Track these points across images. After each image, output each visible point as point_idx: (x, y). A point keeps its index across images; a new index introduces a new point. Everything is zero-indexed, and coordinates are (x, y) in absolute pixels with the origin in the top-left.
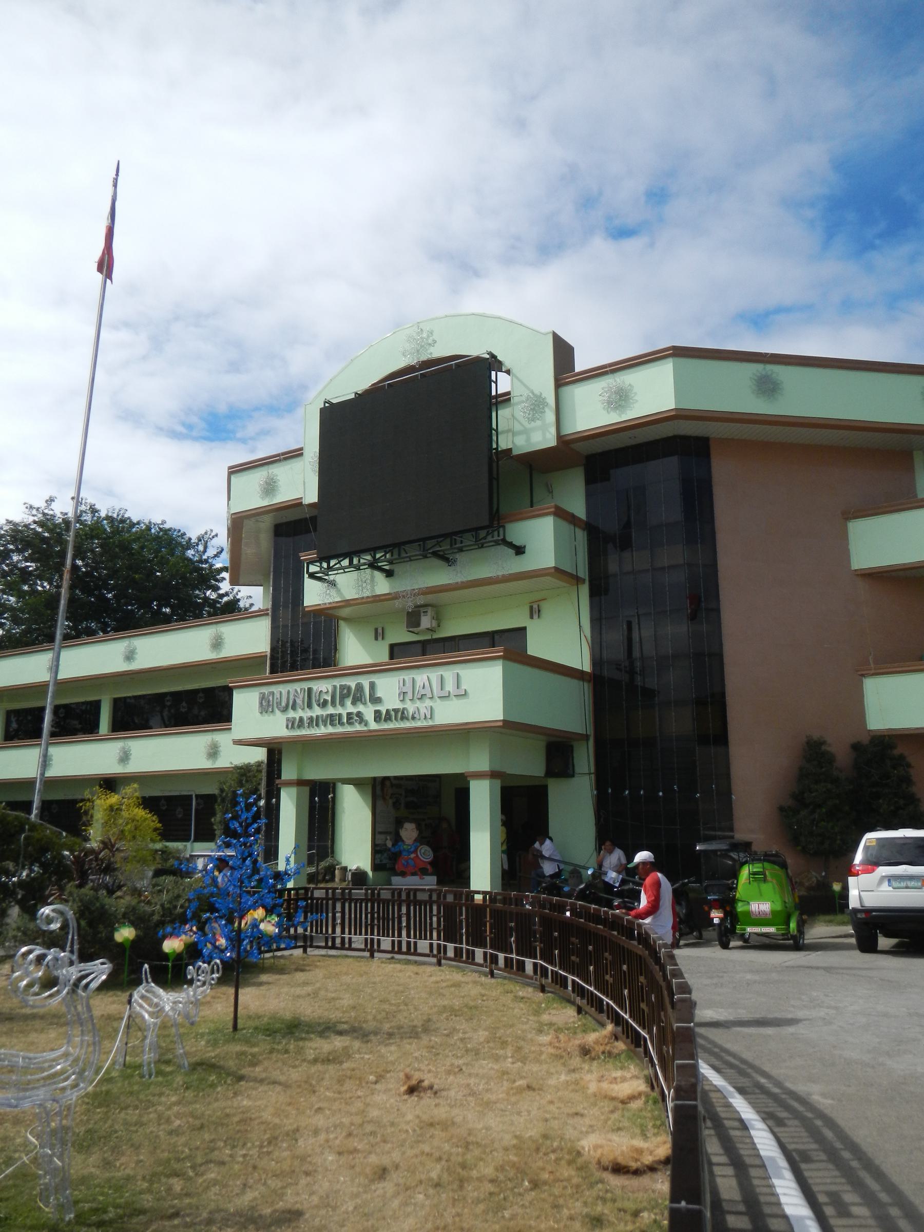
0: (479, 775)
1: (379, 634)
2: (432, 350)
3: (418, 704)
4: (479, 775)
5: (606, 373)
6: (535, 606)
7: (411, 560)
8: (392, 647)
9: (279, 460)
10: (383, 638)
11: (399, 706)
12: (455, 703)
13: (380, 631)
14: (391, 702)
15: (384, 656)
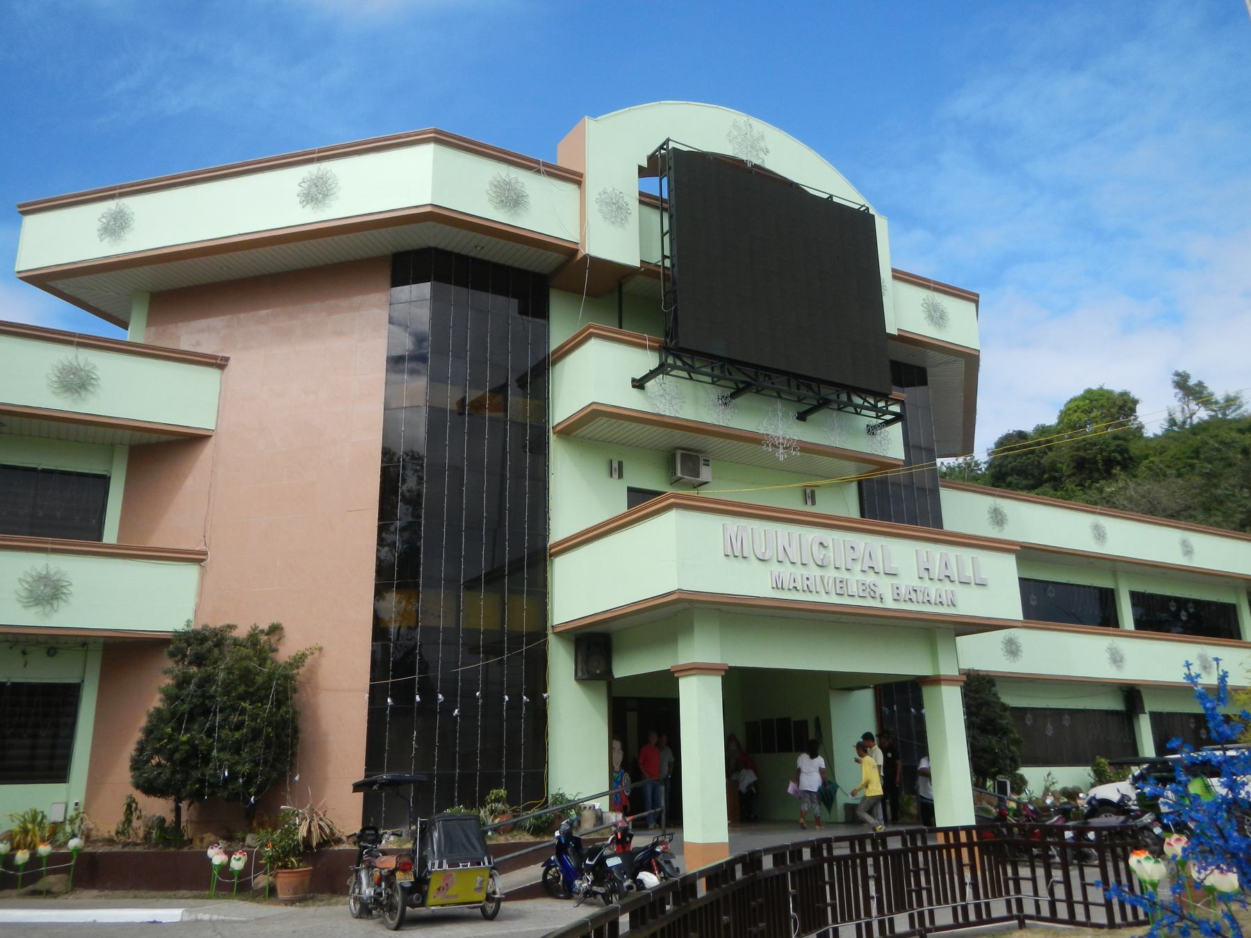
0: (950, 680)
1: (617, 470)
2: (762, 155)
3: (938, 585)
4: (950, 680)
5: (928, 287)
6: (808, 491)
7: (779, 397)
8: (631, 490)
9: (539, 171)
10: (621, 476)
11: (917, 583)
12: (974, 591)
13: (615, 465)
14: (909, 579)
15: (620, 505)
